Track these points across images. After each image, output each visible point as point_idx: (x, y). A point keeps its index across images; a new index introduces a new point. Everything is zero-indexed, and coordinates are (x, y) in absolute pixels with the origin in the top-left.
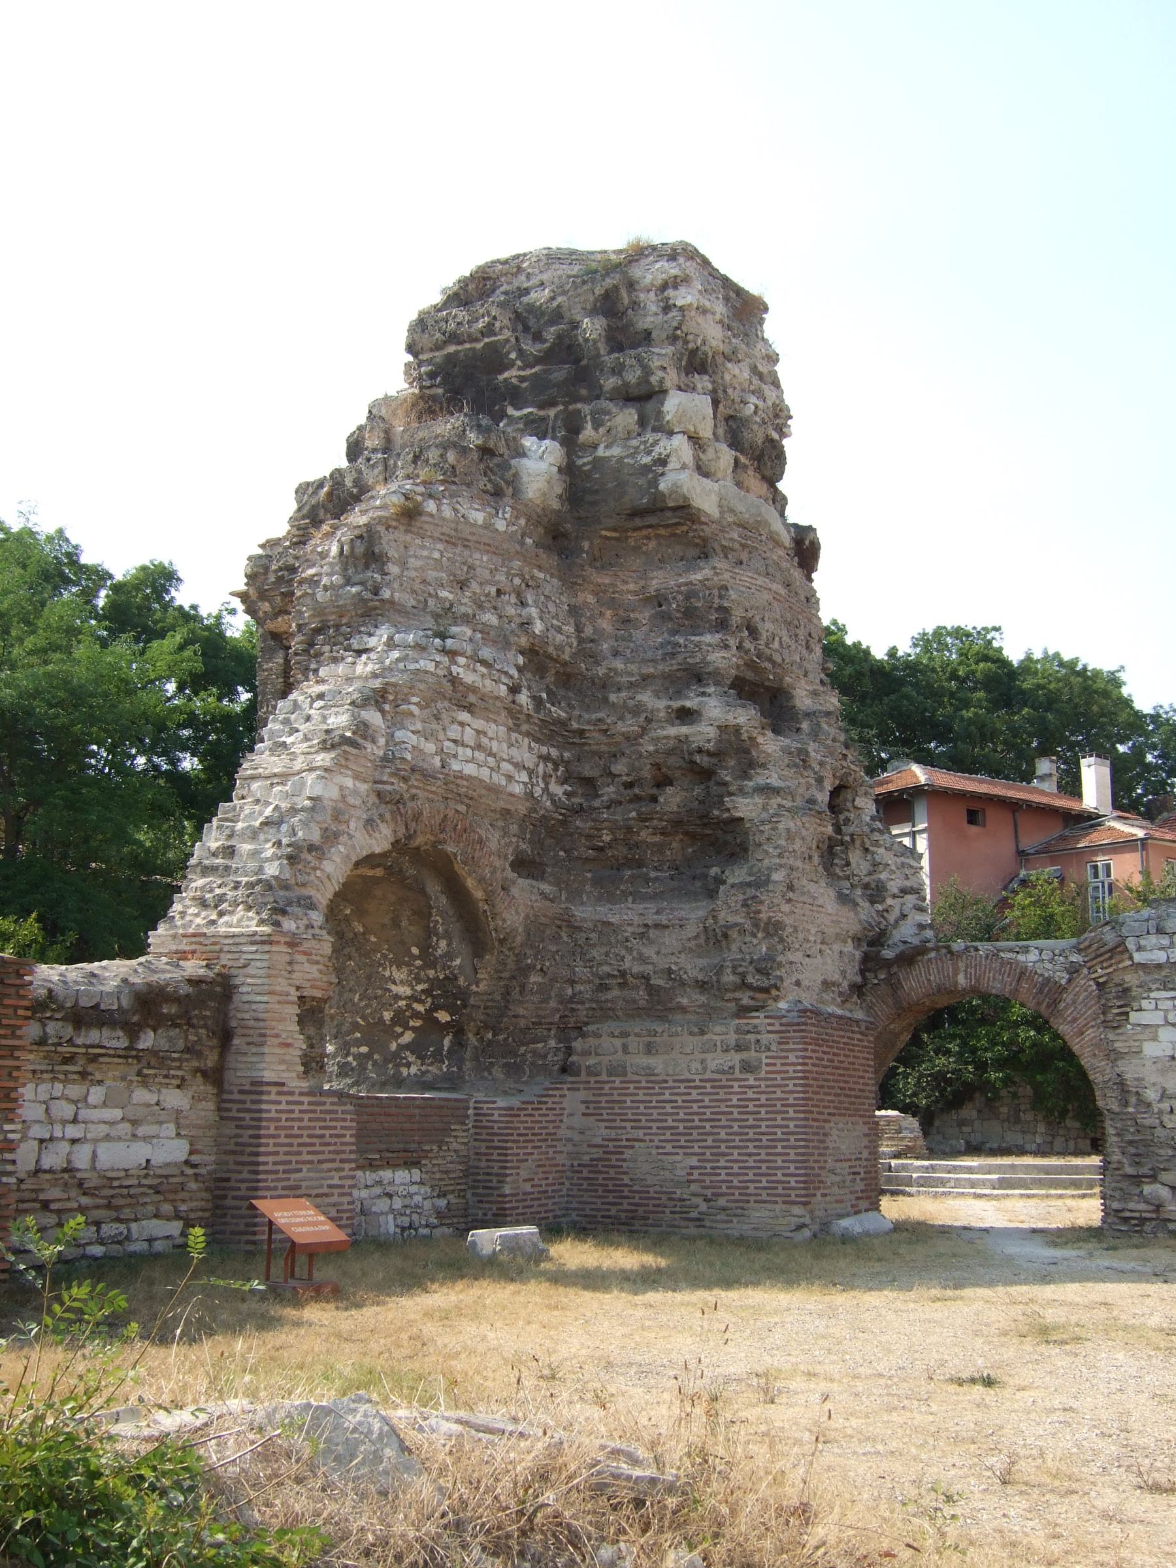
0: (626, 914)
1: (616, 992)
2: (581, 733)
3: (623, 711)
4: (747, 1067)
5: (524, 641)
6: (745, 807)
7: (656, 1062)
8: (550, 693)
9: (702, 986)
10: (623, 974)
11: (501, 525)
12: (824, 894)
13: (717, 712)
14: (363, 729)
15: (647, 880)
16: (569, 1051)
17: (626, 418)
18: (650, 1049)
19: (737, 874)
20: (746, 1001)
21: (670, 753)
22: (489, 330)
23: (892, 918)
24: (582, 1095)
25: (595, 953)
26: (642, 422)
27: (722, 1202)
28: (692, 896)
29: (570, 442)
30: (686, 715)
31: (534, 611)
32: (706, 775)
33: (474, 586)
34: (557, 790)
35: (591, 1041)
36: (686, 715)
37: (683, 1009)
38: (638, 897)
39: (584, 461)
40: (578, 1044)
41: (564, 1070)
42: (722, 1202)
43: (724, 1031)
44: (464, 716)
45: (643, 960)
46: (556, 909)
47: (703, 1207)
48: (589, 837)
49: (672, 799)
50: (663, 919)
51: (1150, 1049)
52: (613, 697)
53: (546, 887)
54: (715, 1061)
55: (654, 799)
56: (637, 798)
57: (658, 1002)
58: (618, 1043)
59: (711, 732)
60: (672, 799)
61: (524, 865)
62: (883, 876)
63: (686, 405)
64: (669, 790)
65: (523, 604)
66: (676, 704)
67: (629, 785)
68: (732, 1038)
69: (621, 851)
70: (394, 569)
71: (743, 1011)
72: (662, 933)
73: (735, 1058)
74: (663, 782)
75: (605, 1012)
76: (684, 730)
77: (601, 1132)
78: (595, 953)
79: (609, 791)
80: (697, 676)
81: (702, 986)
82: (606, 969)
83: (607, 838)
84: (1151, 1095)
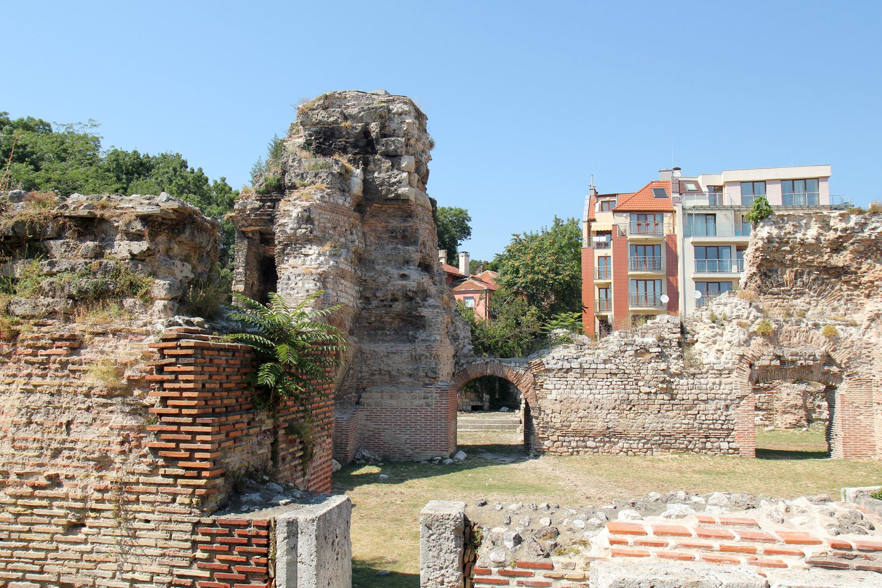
0: (381, 348)
1: (377, 376)
2: (365, 281)
3: (380, 273)
4: (428, 405)
6: (425, 312)
7: (394, 403)
9: (410, 375)
10: (380, 370)
11: (347, 205)
13: (416, 278)
15: (386, 335)
16: (360, 397)
17: (387, 164)
18: (391, 397)
19: (422, 335)
20: (427, 382)
21: (399, 290)
22: (335, 122)
23: (460, 346)
24: (365, 413)
25: (369, 362)
26: (392, 166)
27: (417, 450)
28: (403, 342)
29: (365, 171)
30: (404, 277)
32: (411, 299)
33: (339, 229)
35: (369, 394)
36: (404, 277)
37: (403, 383)
38: (384, 341)
39: (368, 177)
40: (363, 395)
41: (358, 403)
42: (417, 450)
43: (420, 392)
44: (343, 281)
45: (388, 365)
47: (411, 452)
48: (367, 319)
49: (398, 307)
50: (394, 350)
51: (549, 397)
52: (377, 267)
53: (355, 339)
54: (417, 402)
55: (391, 306)
56: (385, 306)
57: (392, 379)
58: (379, 395)
59: (415, 284)
60: (398, 307)
62: (458, 332)
63: (406, 162)
64: (397, 303)
65: (352, 234)
66: (402, 272)
67: (382, 301)
68: (422, 395)
69: (377, 324)
70: (316, 223)
71: (425, 385)
72: (395, 355)
73: (423, 402)
74: (394, 300)
75: (373, 383)
76: (404, 282)
77: (372, 426)
78: (369, 362)
79: (375, 303)
80: (407, 262)
81: (410, 375)
82: (374, 368)
83: (373, 319)
84: (548, 411)
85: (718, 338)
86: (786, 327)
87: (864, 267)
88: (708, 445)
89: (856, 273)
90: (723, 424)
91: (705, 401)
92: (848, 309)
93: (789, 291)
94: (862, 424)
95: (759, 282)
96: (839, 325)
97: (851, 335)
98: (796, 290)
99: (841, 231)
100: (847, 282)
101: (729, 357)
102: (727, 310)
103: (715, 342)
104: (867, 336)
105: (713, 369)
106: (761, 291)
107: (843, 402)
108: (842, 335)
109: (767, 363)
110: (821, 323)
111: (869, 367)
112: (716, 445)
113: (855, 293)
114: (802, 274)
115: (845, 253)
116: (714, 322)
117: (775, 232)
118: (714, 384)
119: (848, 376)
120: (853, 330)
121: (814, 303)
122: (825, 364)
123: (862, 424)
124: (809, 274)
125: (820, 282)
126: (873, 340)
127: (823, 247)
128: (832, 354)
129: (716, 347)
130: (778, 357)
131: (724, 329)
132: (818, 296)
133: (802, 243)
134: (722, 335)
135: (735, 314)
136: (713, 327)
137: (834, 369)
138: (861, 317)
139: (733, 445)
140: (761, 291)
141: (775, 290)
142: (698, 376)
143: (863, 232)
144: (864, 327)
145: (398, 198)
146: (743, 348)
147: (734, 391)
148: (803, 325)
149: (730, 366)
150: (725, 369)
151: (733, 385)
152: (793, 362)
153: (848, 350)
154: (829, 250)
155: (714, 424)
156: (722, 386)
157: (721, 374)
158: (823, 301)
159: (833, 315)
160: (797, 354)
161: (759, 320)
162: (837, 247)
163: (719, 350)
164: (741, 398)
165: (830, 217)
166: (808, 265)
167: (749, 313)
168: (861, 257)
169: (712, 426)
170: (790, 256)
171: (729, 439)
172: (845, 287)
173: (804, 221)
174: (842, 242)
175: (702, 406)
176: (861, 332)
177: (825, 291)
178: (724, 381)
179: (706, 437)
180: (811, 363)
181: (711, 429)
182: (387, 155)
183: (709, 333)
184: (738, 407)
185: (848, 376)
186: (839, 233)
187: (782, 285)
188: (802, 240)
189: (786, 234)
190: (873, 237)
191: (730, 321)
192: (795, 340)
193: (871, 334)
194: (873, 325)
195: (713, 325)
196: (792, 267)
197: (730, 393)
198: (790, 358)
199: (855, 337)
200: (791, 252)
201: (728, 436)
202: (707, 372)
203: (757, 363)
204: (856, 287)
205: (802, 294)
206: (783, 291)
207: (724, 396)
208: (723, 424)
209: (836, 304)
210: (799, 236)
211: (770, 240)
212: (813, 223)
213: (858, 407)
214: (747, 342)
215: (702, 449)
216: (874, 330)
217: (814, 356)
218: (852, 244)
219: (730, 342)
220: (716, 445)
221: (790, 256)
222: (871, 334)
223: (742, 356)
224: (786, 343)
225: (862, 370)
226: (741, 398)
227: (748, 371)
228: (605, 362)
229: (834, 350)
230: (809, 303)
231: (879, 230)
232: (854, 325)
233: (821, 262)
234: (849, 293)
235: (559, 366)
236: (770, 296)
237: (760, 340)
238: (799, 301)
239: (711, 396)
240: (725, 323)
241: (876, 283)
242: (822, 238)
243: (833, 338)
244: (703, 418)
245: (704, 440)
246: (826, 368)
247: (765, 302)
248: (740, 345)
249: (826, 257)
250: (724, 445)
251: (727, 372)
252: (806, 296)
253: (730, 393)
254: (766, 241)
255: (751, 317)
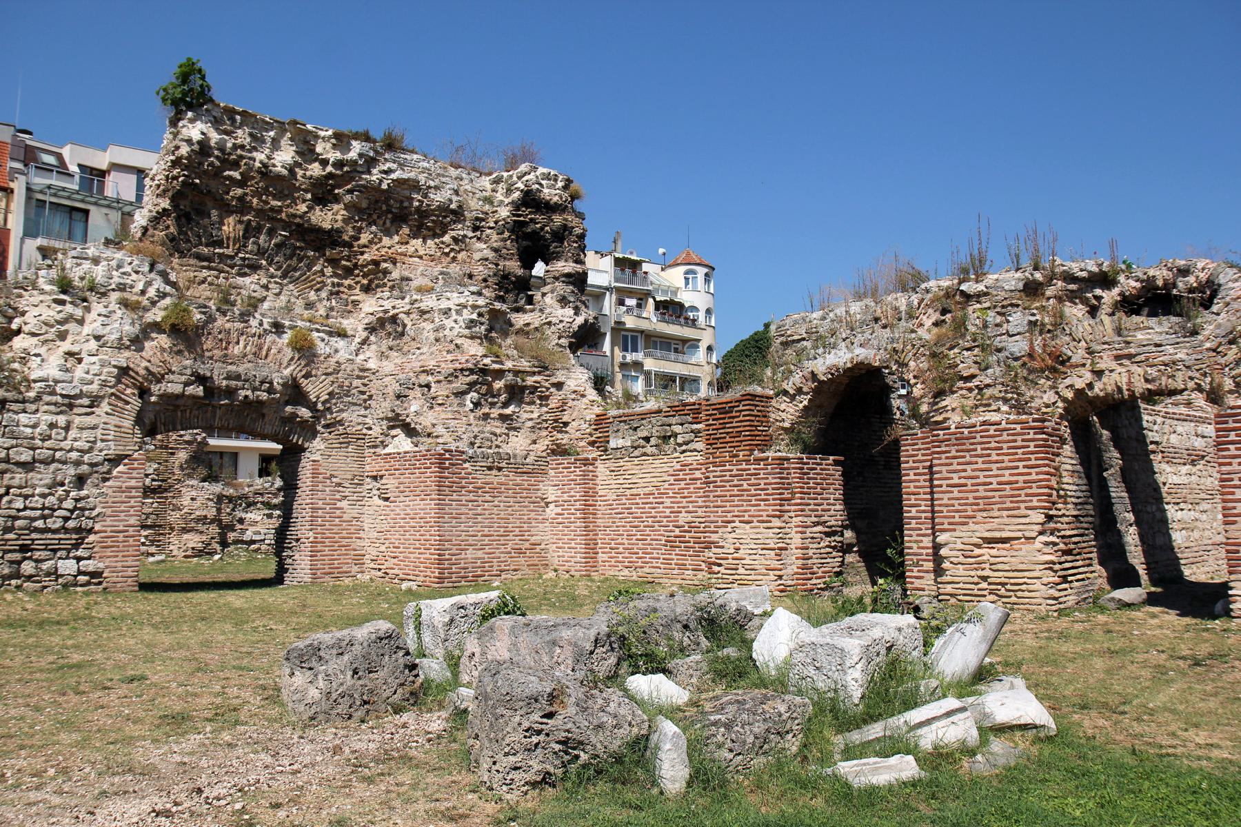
85: (72, 327)
86: (220, 321)
87: (365, 238)
88: (28, 568)
89: (350, 246)
90: (66, 519)
91: (27, 466)
92: (332, 309)
93: (232, 258)
94: (346, 517)
95: (172, 230)
96: (318, 331)
97: (336, 351)
98: (244, 259)
99: (334, 165)
100: (333, 262)
101: (95, 369)
102: (99, 272)
103: (62, 336)
104: (361, 357)
105: (53, 393)
106: (176, 246)
107: (315, 474)
108: (322, 348)
109: (176, 389)
110: (287, 323)
111: (363, 412)
112: (46, 566)
113: (346, 282)
114: (259, 230)
115: (336, 207)
116: (64, 292)
117: (214, 137)
118: (52, 426)
119: (327, 426)
120: (340, 343)
121: (274, 288)
122: (287, 403)
123: (346, 517)
124: (271, 233)
125: (288, 252)
126: (372, 364)
127: (299, 189)
128: (303, 382)
129: (66, 346)
130: (201, 379)
131: (88, 309)
132: (284, 276)
133: (265, 172)
134: (81, 322)
135: (116, 280)
136: (63, 303)
137: (304, 413)
138: (354, 325)
139: (89, 565)
140: (176, 246)
142: (15, 407)
143: (369, 173)
144: (358, 340)
146: (127, 354)
147: (99, 445)
148: (254, 323)
149: (94, 388)
150: (81, 395)
151: (99, 432)
152: (231, 392)
153: (331, 378)
154: (309, 196)
155: (44, 517)
156: (73, 433)
157: (71, 406)
158: (291, 287)
159: (307, 314)
160: (238, 377)
161: (168, 301)
162: (323, 193)
163: (70, 354)
164: (116, 461)
165: (317, 137)
166: (269, 215)
167: (149, 284)
168: (361, 220)
169: (39, 524)
170: (239, 191)
171: (79, 553)
172: (329, 271)
173: (272, 134)
174: (334, 187)
175: (19, 477)
176: (353, 347)
177: (295, 270)
178: (77, 420)
179: (24, 549)
180: (264, 396)
181: (37, 530)
183: (52, 313)
184: (105, 480)
185: (327, 426)
186: (329, 169)
187: (219, 243)
188: (265, 165)
189: (235, 147)
190: (384, 186)
191: (104, 294)
192: (237, 350)
193: (368, 354)
194: (372, 338)
195: (62, 297)
196: (243, 214)
197: (90, 450)
198: (225, 383)
199: (343, 356)
200: (242, 183)
201: (76, 546)
202: (38, 398)
203: (155, 388)
204: (349, 272)
205: (255, 268)
206: (221, 256)
207: (74, 455)
208: (66, 519)
209: (312, 296)
210: (260, 156)
211: (204, 147)
212: (285, 141)
213: (339, 485)
214: (137, 342)
215: (10, 577)
216: (373, 347)
217: (271, 383)
218: (350, 192)
219: (98, 338)
220: (46, 566)
221: (239, 191)
222: (368, 354)
223: (124, 371)
224: (217, 353)
225: (351, 416)
226: (116, 461)
227: (136, 403)
229: (306, 376)
231: (394, 176)
232: (342, 334)
233: (295, 216)
234: (336, 280)
236: (192, 261)
237: (164, 340)
238: (248, 280)
239: (43, 453)
240: (93, 298)
241: (384, 265)
242: (300, 172)
243: (304, 350)
244: (19, 504)
245: (17, 556)
246: (289, 409)
247: (181, 271)
248: (120, 346)
249: (303, 208)
250: (68, 567)
251: (86, 401)
252: (261, 272)
253: (90, 450)
254: (196, 147)
255: (152, 292)
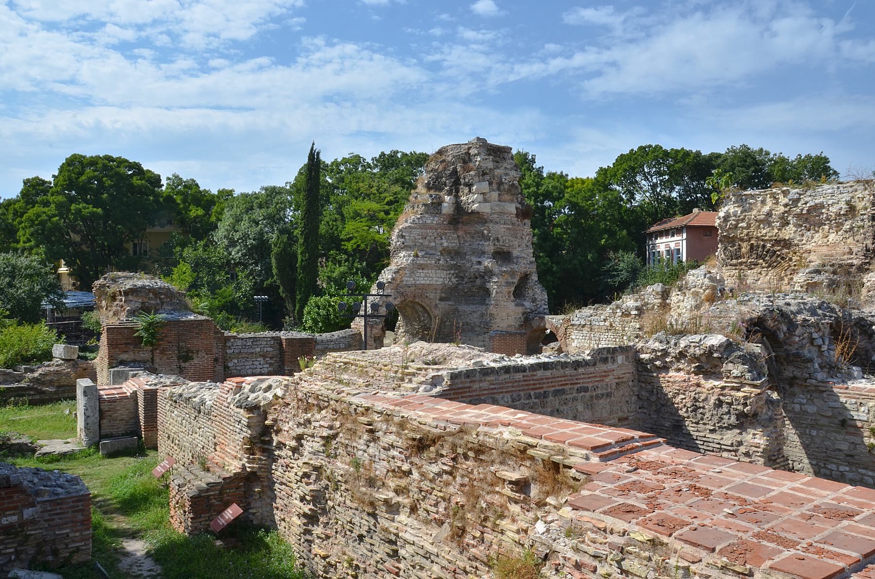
0: (468, 309)
3: (468, 261)
5: (441, 249)
8: (452, 257)
12: (511, 306)
14: (393, 279)
17: (466, 190)
31: (444, 241)
34: (454, 280)
46: (453, 308)
53: (451, 303)
61: (441, 299)
79: (466, 280)
141: (734, 261)
145: (473, 212)
154: (778, 224)
170: (745, 231)
182: (466, 185)
187: (740, 257)
228: (605, 320)
230: (760, 273)
235: (578, 323)
